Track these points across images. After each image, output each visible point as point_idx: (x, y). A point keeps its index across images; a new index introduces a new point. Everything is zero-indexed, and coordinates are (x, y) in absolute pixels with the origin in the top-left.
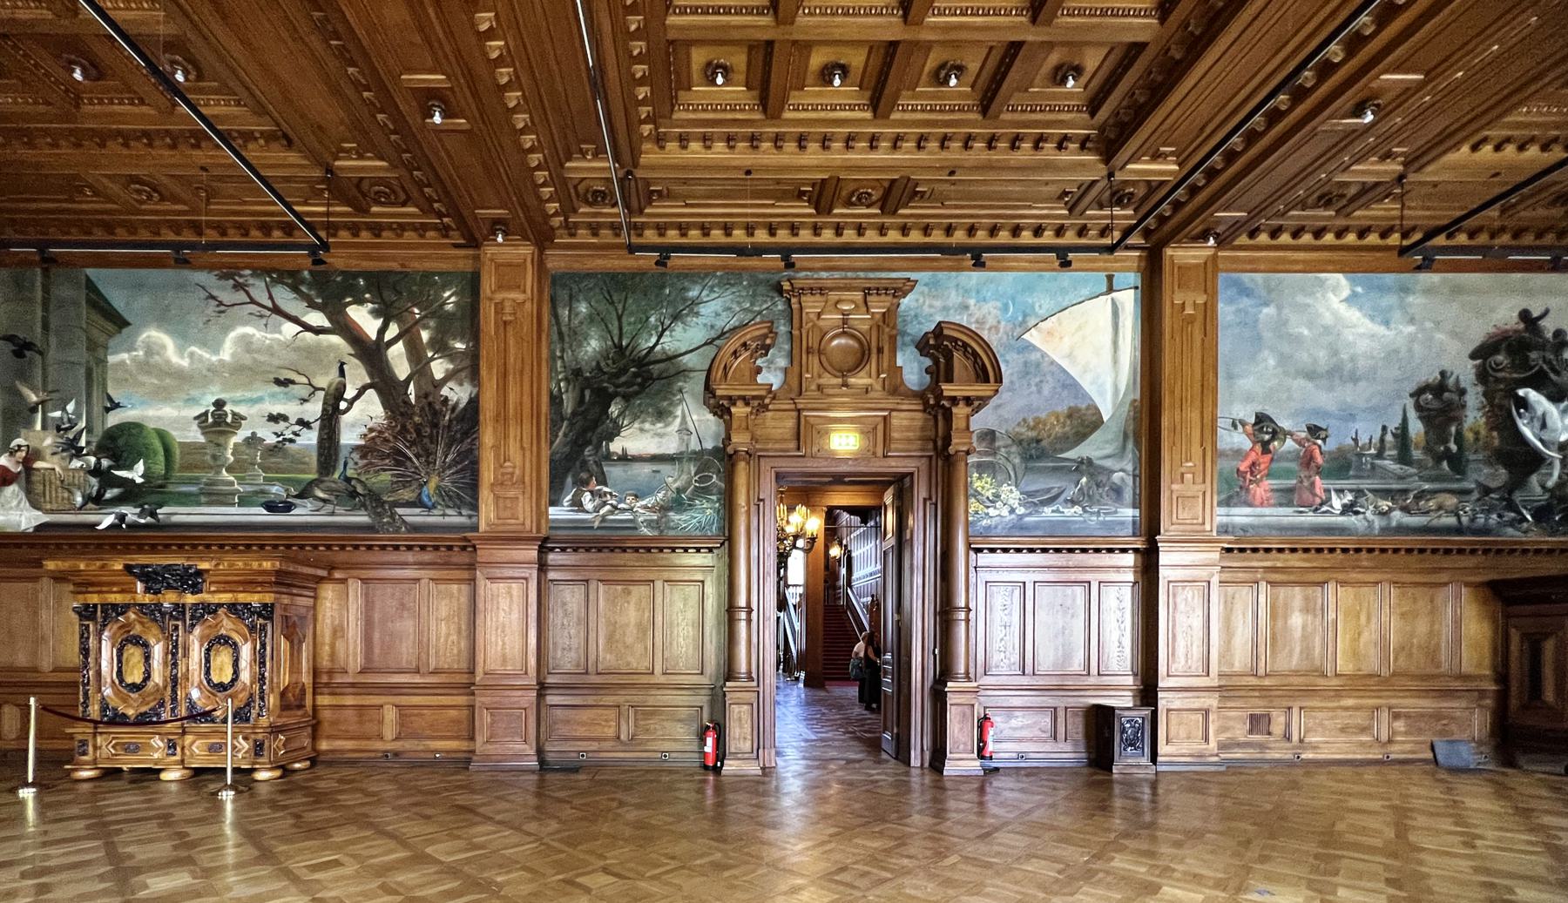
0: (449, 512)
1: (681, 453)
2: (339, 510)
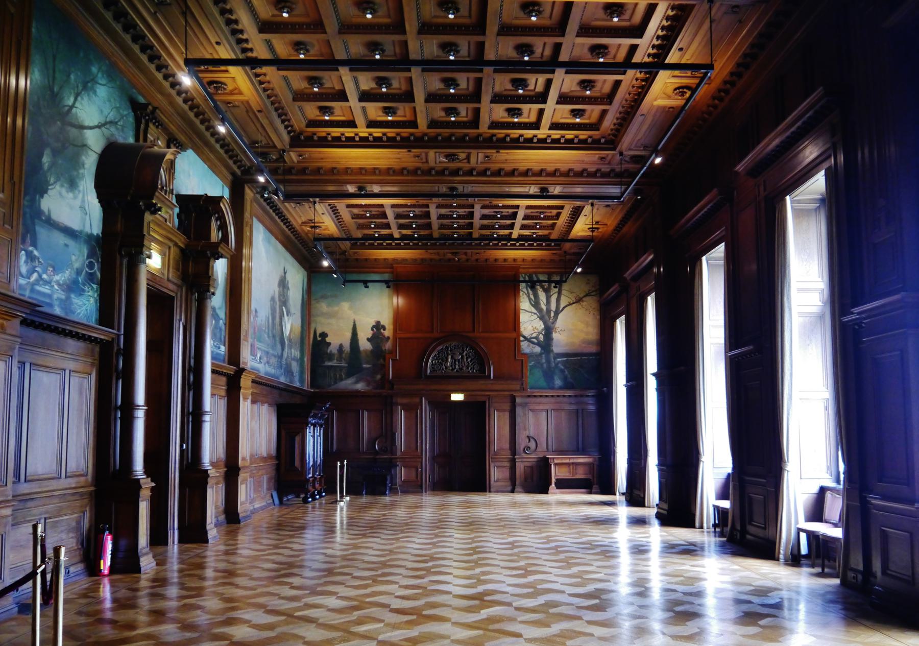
1: (81, 232)
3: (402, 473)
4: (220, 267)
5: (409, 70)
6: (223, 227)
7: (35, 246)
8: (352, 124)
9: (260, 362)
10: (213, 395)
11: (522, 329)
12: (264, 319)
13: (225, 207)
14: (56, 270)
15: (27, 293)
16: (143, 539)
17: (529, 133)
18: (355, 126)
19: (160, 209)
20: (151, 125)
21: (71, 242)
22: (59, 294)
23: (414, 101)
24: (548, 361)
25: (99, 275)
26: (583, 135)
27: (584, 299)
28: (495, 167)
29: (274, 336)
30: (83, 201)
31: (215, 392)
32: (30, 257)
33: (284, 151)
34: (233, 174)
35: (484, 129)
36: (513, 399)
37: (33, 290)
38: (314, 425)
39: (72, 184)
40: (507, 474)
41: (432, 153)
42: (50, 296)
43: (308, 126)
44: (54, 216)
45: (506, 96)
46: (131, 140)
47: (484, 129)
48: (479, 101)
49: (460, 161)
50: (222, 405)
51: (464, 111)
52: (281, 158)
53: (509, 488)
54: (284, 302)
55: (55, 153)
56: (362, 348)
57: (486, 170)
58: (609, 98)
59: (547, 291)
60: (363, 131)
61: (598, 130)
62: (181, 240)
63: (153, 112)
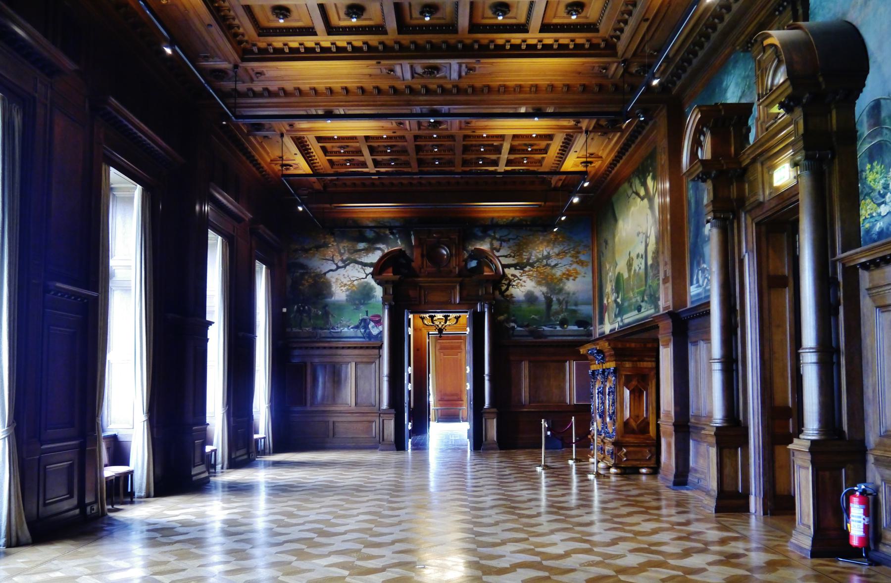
8: (310, 31)
17: (516, 38)
18: (315, 34)
26: (580, 38)
43: (259, 35)
60: (326, 41)
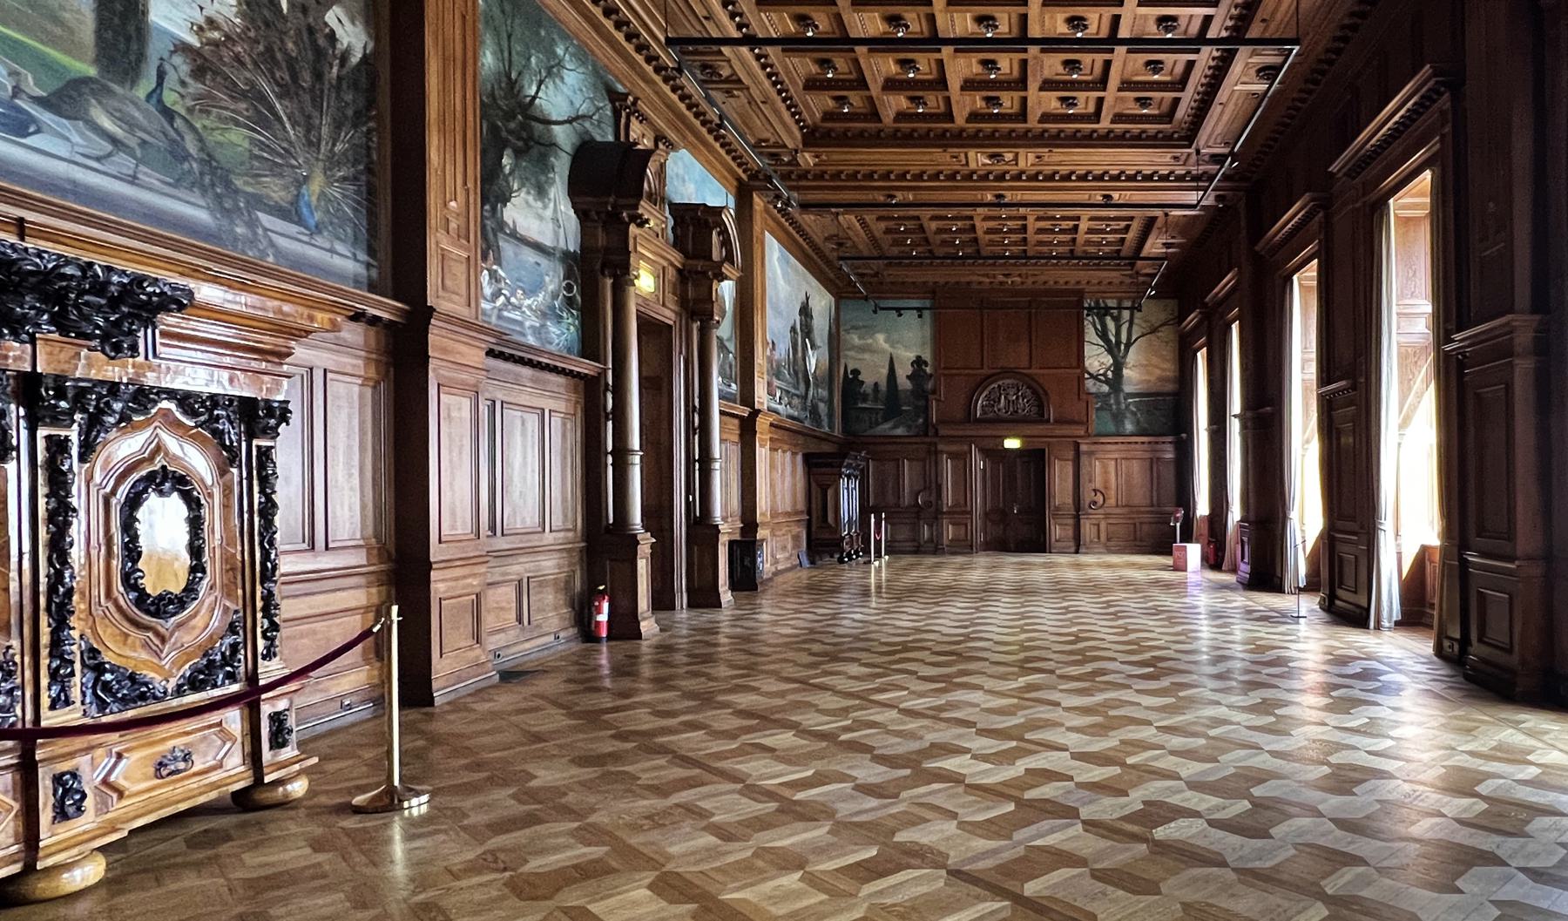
0: (339, 247)
2: (147, 175)
3: (950, 532)
4: (726, 290)
5: (939, 51)
6: (726, 243)
7: (500, 265)
9: (780, 403)
10: (722, 441)
11: (1087, 363)
12: (783, 353)
13: (728, 219)
14: (529, 293)
15: (494, 320)
16: (643, 603)
19: (647, 221)
20: (633, 119)
21: (544, 262)
22: (532, 321)
23: (947, 89)
24: (1118, 403)
25: (579, 298)
27: (1162, 329)
28: (1048, 170)
29: (796, 373)
30: (555, 210)
31: (724, 437)
32: (494, 276)
33: (796, 151)
34: (739, 179)
35: (1033, 122)
36: (1077, 445)
37: (500, 317)
38: (849, 477)
39: (541, 192)
40: (1070, 532)
41: (972, 153)
42: (521, 324)
44: (521, 230)
45: (1058, 82)
46: (611, 138)
47: (1033, 122)
48: (1025, 89)
49: (1007, 163)
50: (735, 452)
51: (1009, 101)
52: (794, 162)
53: (1073, 550)
54: (807, 331)
55: (518, 154)
56: (900, 388)
57: (1038, 173)
58: (1181, 83)
59: (1117, 319)
61: (1170, 122)
62: (676, 257)
63: (634, 103)
